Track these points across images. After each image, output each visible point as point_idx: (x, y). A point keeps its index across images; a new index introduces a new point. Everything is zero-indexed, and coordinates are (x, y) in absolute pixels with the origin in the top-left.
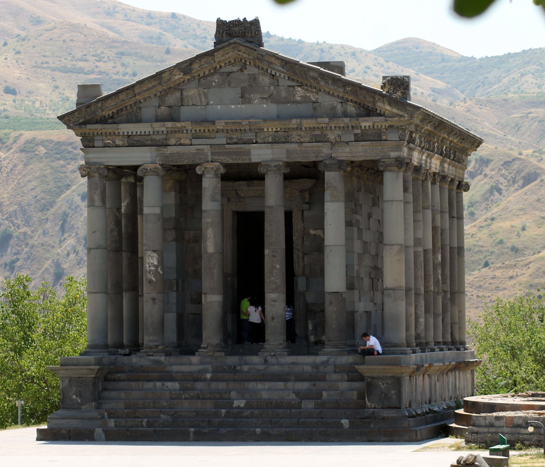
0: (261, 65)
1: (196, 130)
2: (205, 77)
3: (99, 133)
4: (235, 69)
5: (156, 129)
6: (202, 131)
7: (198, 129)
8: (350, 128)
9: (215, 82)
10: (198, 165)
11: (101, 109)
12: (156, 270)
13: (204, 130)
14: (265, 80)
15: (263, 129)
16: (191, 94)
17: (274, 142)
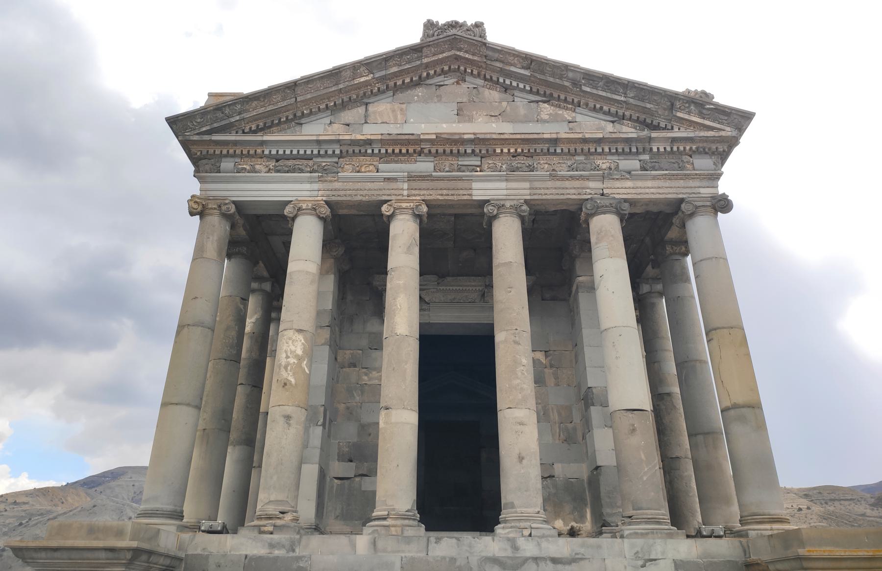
1: (387, 151)
2: (405, 87)
3: (231, 151)
4: (450, 81)
6: (397, 151)
7: (390, 151)
8: (634, 150)
9: (418, 96)
10: (386, 201)
12: (299, 365)
13: (400, 151)
14: (493, 95)
15: (495, 151)
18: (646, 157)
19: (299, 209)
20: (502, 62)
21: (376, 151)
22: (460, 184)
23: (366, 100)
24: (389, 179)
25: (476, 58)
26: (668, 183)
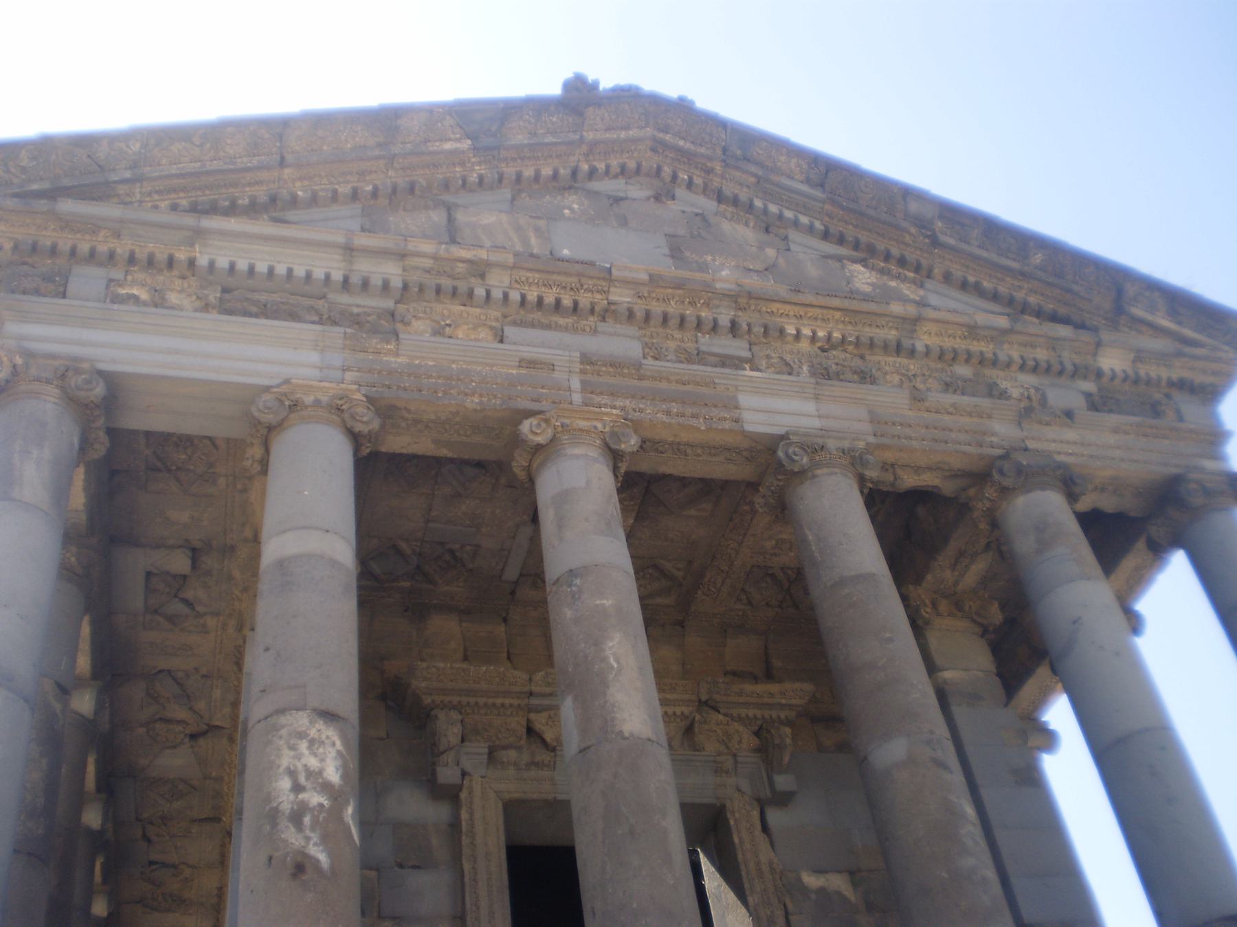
0: (729, 189)
1: (523, 297)
4: (637, 191)
5: (364, 267)
7: (532, 296)
8: (1069, 367)
10: (530, 414)
15: (782, 331)
16: (486, 221)
17: (824, 374)
18: (1089, 386)
19: (295, 406)
20: (757, 163)
21: (497, 294)
23: (446, 197)
24: (531, 364)
25: (703, 150)
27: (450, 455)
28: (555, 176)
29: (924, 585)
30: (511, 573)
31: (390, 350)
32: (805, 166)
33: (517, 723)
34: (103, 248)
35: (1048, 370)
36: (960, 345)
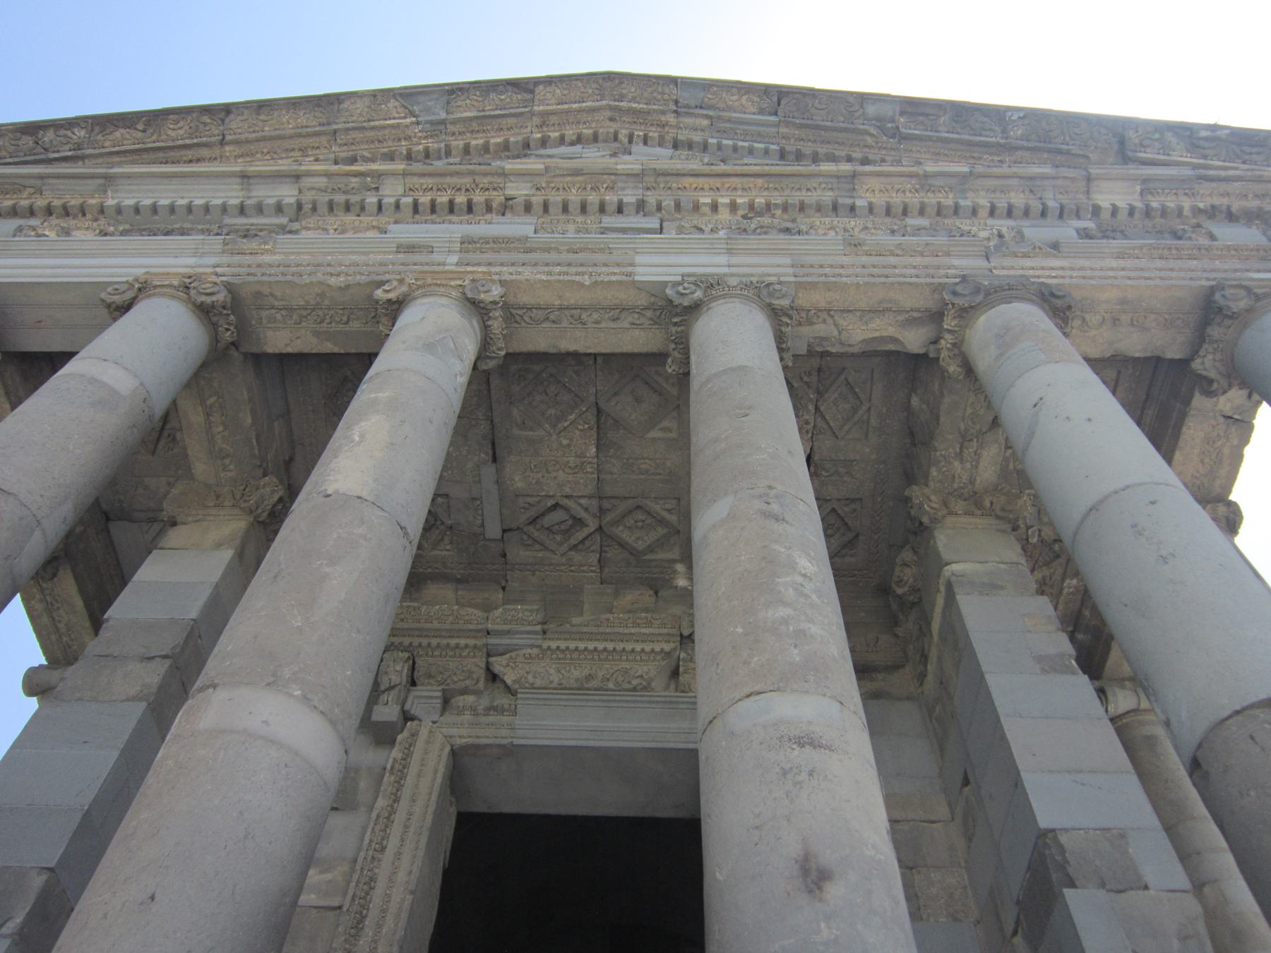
7: (425, 199)
11: (79, 147)
15: (696, 207)
20: (710, 108)
22: (599, 257)
24: (411, 248)
26: (1159, 263)
27: (336, 350)
28: (506, 146)
29: (931, 484)
30: (493, 530)
31: (267, 251)
32: (756, 99)
33: (476, 664)
34: (25, 203)
35: (1026, 213)
36: (913, 200)
